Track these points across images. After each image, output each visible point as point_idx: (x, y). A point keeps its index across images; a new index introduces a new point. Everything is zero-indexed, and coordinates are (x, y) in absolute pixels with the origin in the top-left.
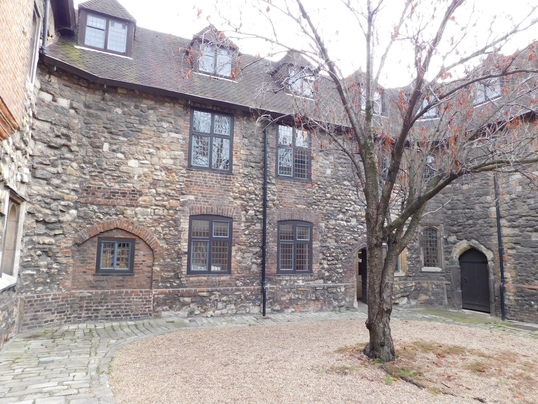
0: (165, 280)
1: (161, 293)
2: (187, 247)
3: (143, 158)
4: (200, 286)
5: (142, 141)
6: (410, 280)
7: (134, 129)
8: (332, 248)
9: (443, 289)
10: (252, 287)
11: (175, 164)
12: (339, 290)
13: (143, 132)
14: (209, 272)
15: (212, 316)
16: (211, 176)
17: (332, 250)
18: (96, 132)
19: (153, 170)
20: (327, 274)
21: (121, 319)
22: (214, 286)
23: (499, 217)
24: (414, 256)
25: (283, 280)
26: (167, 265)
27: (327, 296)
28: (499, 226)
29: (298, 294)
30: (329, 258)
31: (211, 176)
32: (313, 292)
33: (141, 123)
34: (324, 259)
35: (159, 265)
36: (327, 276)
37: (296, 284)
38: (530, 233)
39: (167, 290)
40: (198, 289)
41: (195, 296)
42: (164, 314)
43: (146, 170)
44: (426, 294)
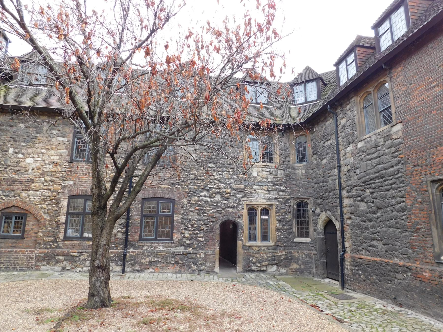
0: (46, 243)
1: (42, 253)
2: (65, 219)
3: (37, 156)
4: (73, 248)
5: (37, 145)
6: (280, 249)
7: (32, 137)
8: (194, 220)
9: (311, 258)
10: (116, 251)
11: (60, 159)
12: (198, 256)
13: (38, 138)
14: (81, 238)
15: (80, 271)
16: (87, 167)
17: (193, 222)
18: (5, 141)
19: (44, 164)
20: (188, 242)
21: (10, 271)
22: (85, 249)
23: (341, 189)
24: (285, 227)
25: (145, 246)
26: (49, 232)
27: (186, 260)
28: (341, 198)
29: (158, 258)
30: (190, 229)
31: (87, 167)
32: (173, 257)
33: (37, 133)
34: (185, 229)
35: (42, 232)
36: (188, 244)
37: (157, 249)
38: (358, 203)
39: (46, 251)
40: (70, 251)
41: (68, 256)
42: (43, 268)
43: (38, 165)
44: (297, 263)
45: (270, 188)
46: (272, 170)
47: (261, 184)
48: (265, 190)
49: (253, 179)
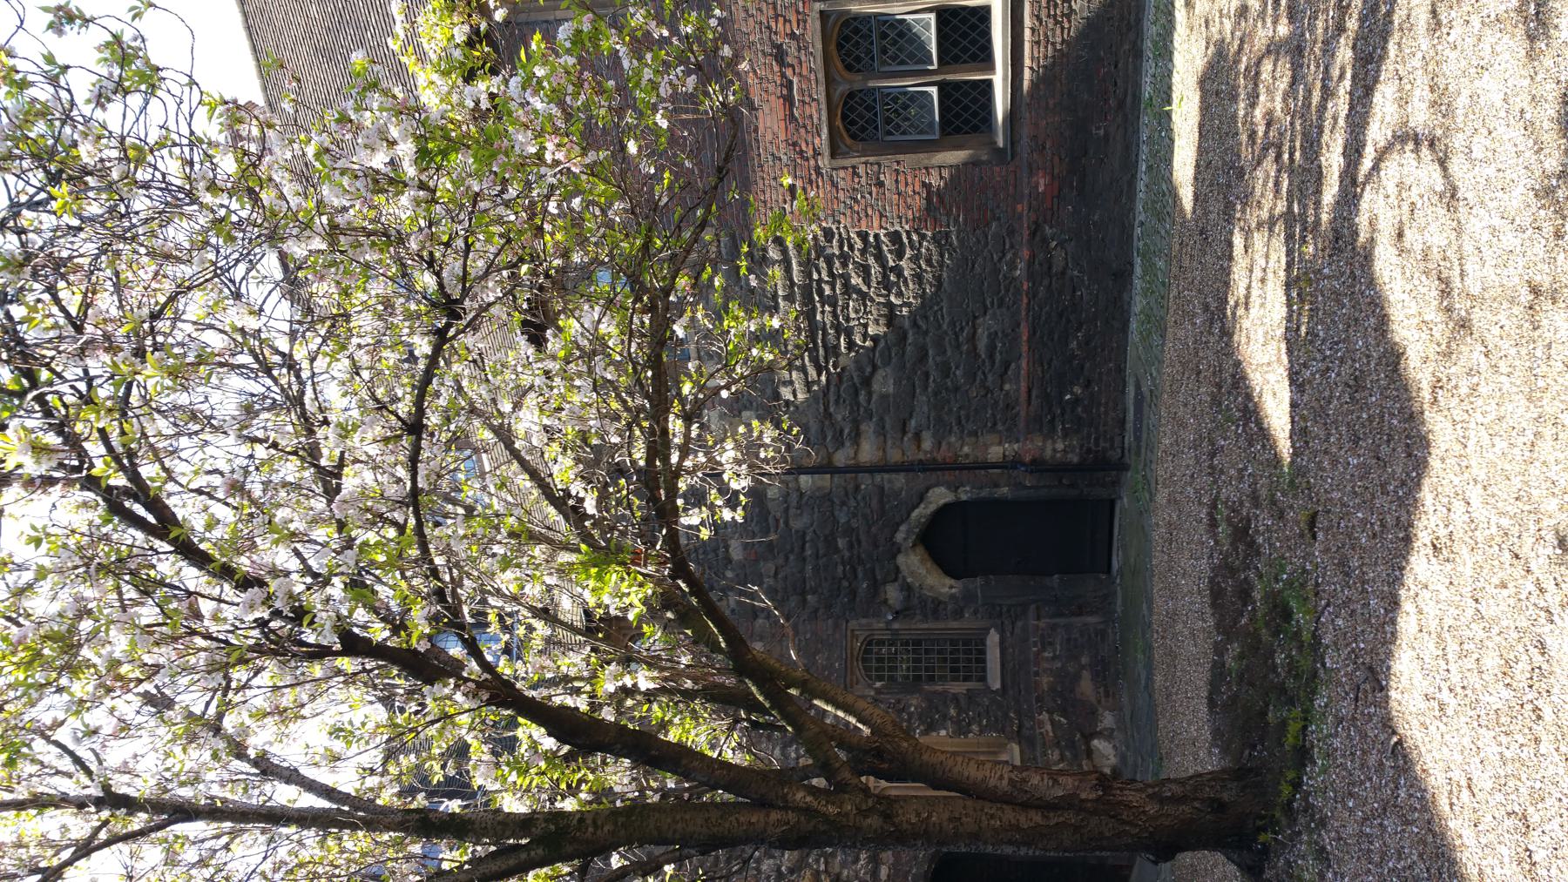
6: (1032, 728)
9: (1054, 627)
24: (953, 712)
28: (857, 469)
38: (875, 397)
44: (1077, 677)
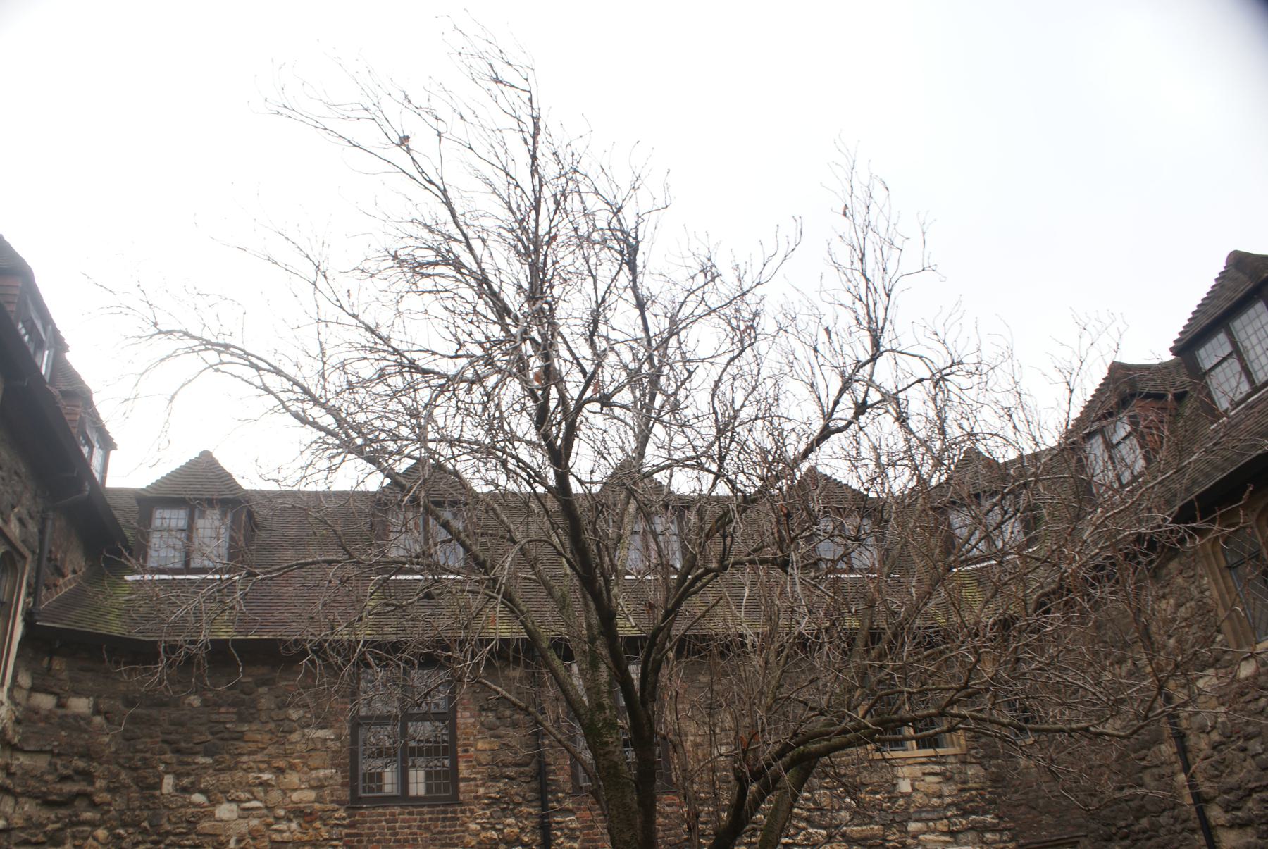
3: (248, 795)
5: (245, 758)
7: (226, 735)
11: (319, 799)
13: (246, 738)
16: (406, 816)
18: (148, 755)
19: (271, 820)
31: (406, 816)
33: (242, 719)
43: (254, 822)
45: (955, 824)
46: (949, 767)
47: (929, 816)
48: (943, 833)
49: (901, 801)
